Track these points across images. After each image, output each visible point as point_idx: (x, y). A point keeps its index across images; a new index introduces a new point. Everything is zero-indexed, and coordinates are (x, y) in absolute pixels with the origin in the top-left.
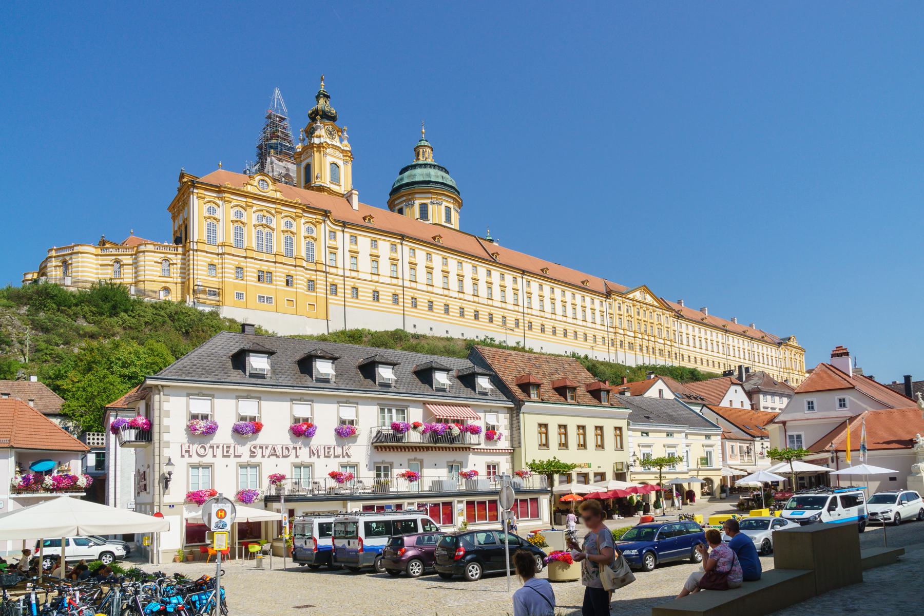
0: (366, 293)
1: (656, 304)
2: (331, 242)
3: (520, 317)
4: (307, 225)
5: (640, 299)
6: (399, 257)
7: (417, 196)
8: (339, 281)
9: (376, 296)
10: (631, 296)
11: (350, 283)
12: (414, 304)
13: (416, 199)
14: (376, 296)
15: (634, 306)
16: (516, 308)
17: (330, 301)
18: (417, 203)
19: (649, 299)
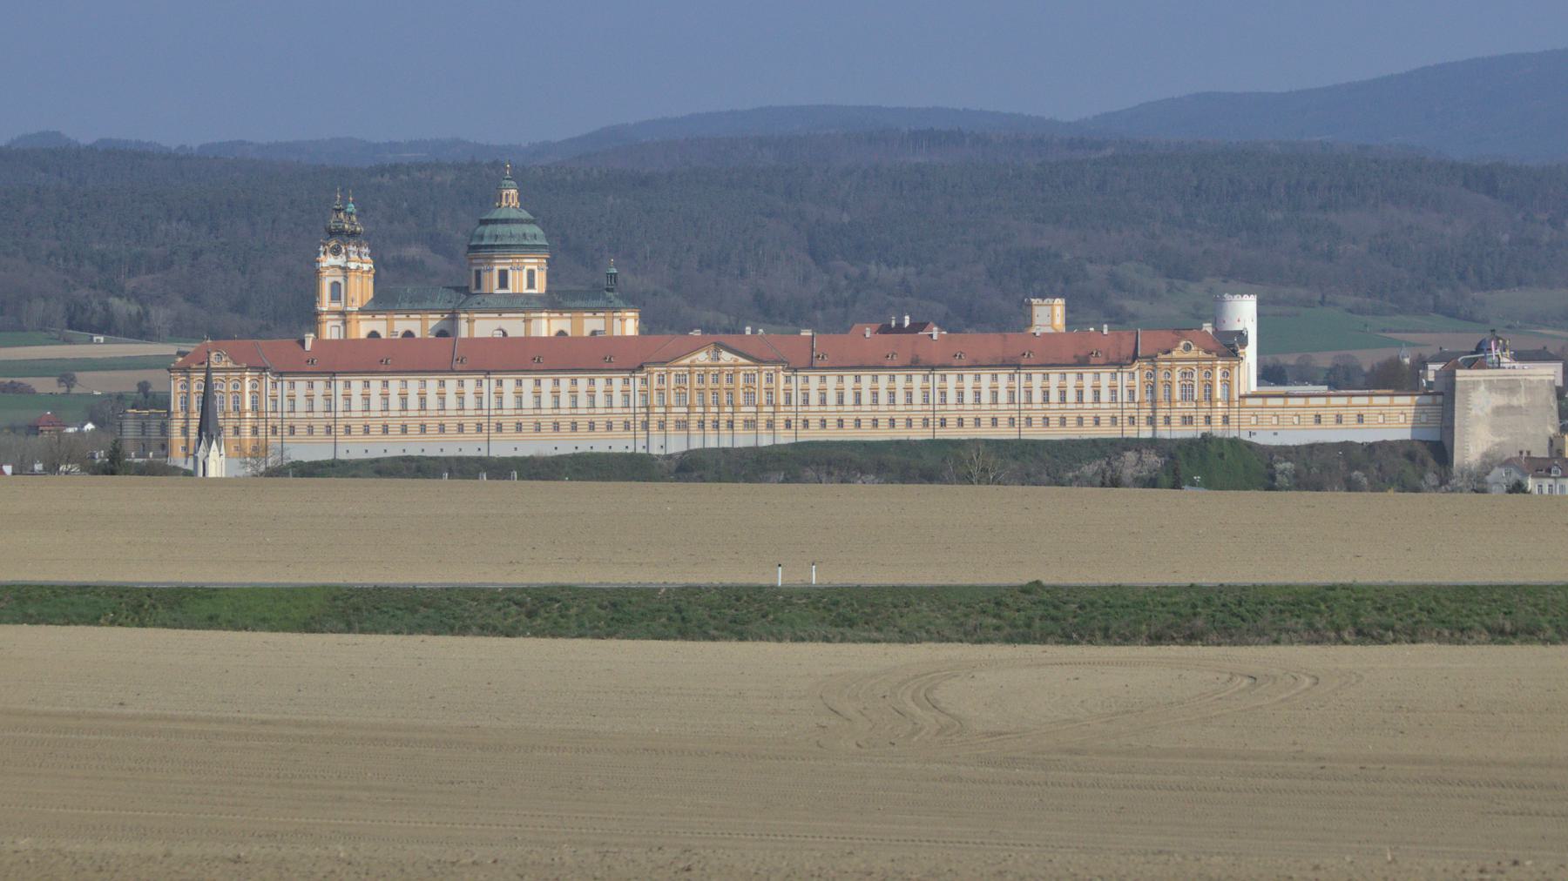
0: (301, 430)
1: (742, 360)
2: (274, 392)
3: (484, 421)
4: (253, 382)
5: (707, 362)
6: (333, 394)
7: (497, 261)
8: (278, 423)
9: (311, 430)
10: (687, 361)
11: (287, 423)
12: (348, 430)
13: (495, 264)
14: (311, 430)
15: (690, 373)
16: (479, 412)
17: (269, 441)
18: (497, 268)
19: (726, 357)
